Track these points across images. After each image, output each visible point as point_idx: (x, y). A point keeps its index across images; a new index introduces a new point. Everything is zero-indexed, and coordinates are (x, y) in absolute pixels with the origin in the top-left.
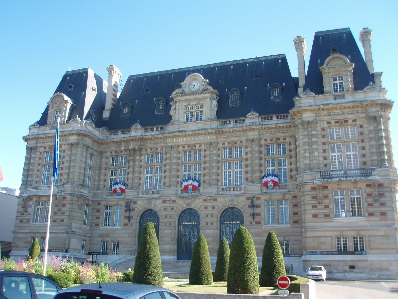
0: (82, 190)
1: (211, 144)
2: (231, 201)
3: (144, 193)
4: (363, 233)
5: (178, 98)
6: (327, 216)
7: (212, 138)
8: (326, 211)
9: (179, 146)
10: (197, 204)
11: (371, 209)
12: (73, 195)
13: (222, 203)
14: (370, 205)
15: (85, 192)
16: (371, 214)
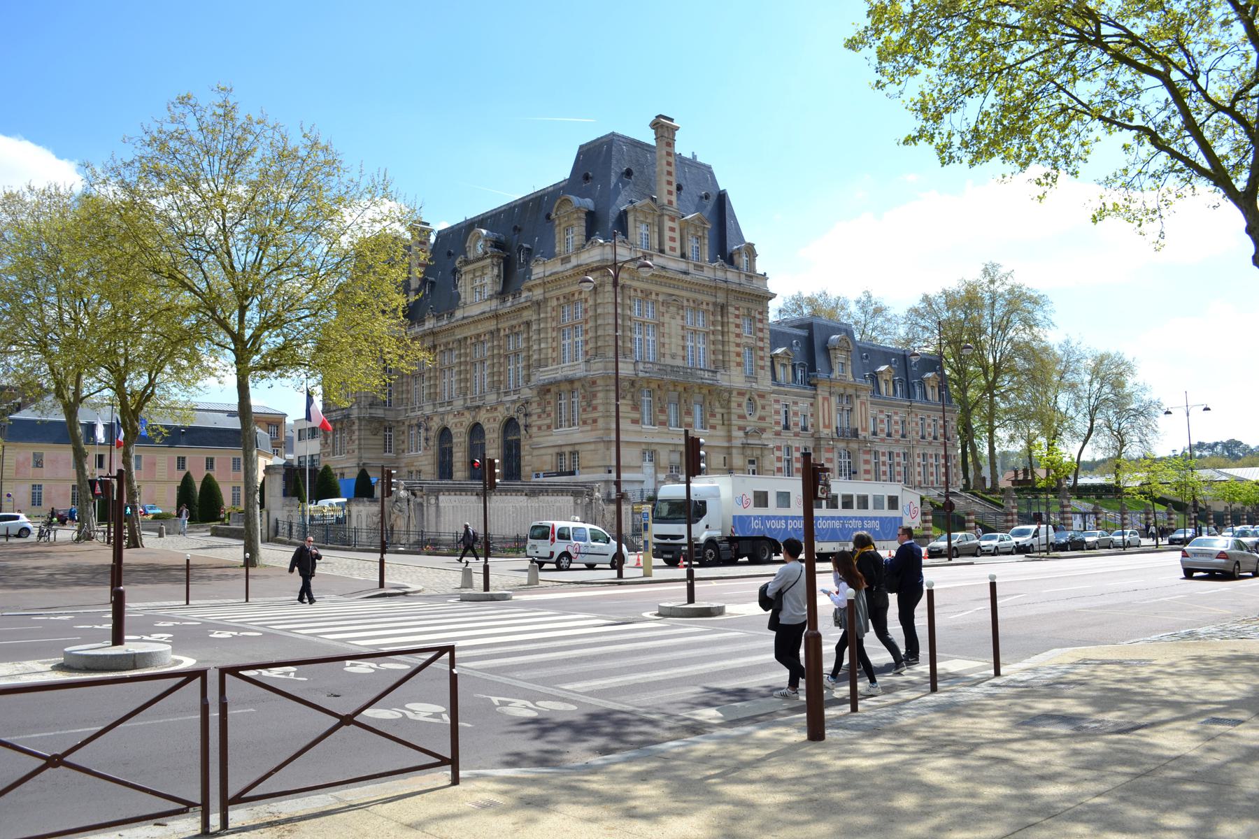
0: (373, 411)
1: (492, 333)
2: (508, 409)
3: (442, 405)
4: (577, 448)
5: (464, 269)
6: (549, 427)
7: (491, 325)
8: (548, 421)
9: (466, 338)
10: (482, 417)
11: (584, 416)
12: (359, 418)
13: (501, 414)
14: (584, 410)
15: (379, 412)
16: (585, 423)
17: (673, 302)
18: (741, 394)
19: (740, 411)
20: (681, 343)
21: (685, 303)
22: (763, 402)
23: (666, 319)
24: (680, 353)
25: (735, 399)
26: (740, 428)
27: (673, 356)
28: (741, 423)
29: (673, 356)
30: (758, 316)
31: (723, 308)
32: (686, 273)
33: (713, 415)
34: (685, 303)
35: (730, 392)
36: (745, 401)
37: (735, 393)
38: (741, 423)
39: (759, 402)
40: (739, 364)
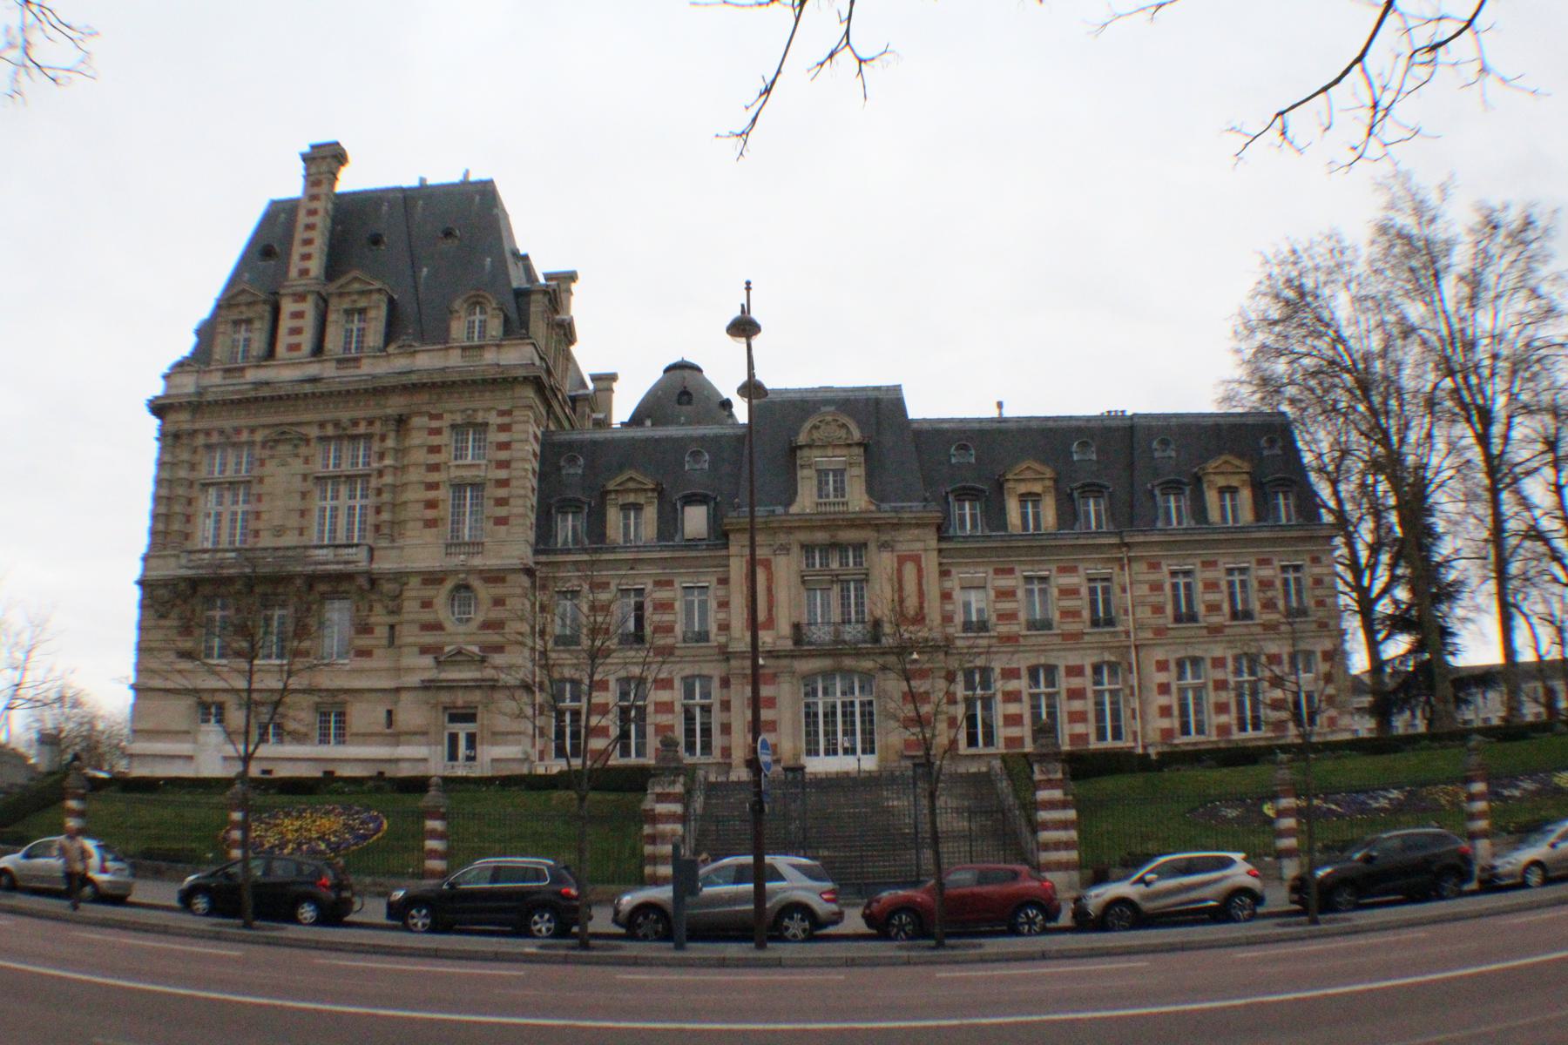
17: (281, 437)
18: (432, 578)
19: (427, 616)
20: (296, 503)
21: (314, 432)
22: (498, 590)
23: (271, 467)
24: (294, 521)
25: (414, 590)
26: (424, 650)
27: (279, 531)
28: (429, 638)
29: (279, 531)
30: (494, 419)
31: (401, 422)
32: (314, 380)
33: (365, 629)
34: (314, 432)
35: (400, 577)
36: (441, 595)
37: (414, 582)
38: (429, 638)
39: (484, 592)
40: (431, 524)
